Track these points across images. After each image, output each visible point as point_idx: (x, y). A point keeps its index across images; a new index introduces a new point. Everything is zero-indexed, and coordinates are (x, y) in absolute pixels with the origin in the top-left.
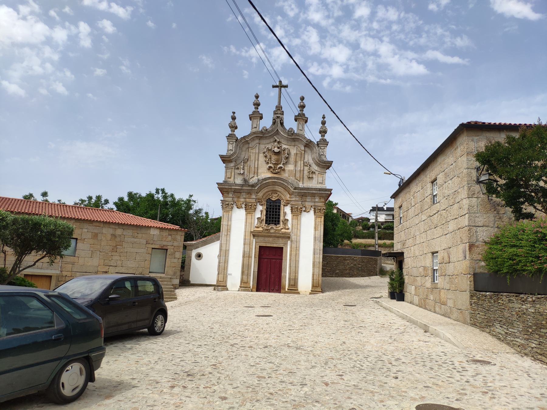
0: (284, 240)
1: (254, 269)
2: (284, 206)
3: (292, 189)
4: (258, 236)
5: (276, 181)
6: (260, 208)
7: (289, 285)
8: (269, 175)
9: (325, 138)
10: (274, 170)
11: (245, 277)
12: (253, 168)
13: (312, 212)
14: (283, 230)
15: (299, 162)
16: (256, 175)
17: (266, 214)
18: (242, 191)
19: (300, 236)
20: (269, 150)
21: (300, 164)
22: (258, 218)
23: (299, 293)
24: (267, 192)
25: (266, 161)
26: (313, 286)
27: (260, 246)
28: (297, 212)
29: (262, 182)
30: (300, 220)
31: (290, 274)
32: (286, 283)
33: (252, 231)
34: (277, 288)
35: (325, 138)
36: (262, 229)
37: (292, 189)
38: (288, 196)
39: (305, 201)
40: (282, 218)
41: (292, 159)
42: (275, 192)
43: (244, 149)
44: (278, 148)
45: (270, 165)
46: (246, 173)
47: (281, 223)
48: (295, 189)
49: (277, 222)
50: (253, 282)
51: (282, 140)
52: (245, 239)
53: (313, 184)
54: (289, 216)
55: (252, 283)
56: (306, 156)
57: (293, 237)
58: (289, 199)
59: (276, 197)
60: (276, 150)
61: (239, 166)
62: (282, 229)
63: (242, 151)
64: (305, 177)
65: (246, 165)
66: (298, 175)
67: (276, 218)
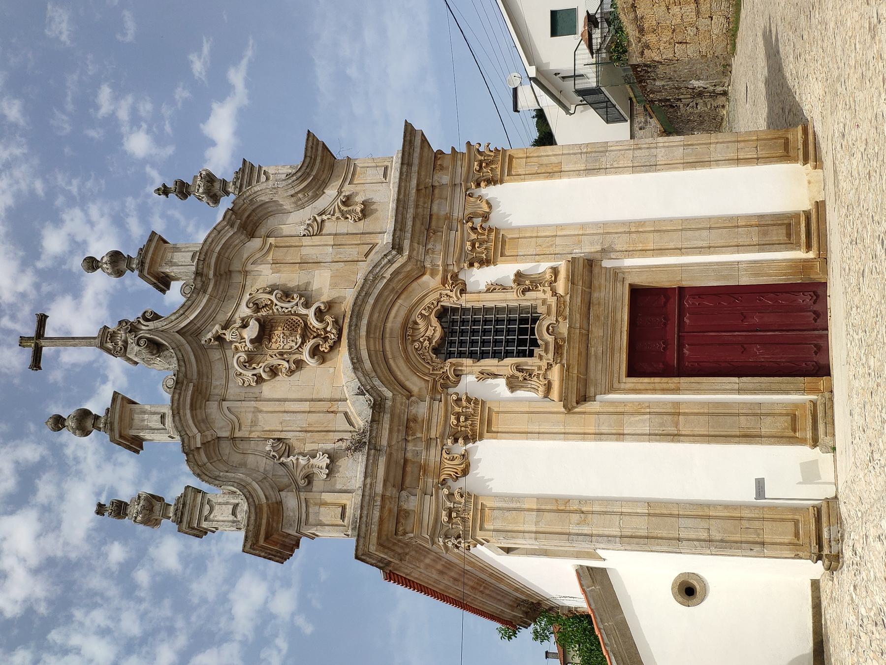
0: (601, 281)
2: (463, 291)
3: (401, 260)
5: (365, 322)
6: (469, 384)
7: (790, 243)
8: (343, 356)
9: (230, 178)
10: (326, 339)
11: (767, 426)
12: (313, 418)
13: (489, 192)
14: (561, 286)
15: (304, 251)
16: (341, 407)
17: (496, 355)
18: (398, 456)
19: (583, 226)
20: (250, 360)
21: (312, 248)
22: (512, 385)
23: (820, 206)
24: (407, 359)
25: (291, 372)
26: (786, 154)
27: (631, 373)
28: (488, 245)
29: (365, 374)
30: (519, 229)
31: (739, 247)
32: (775, 261)
34: (804, 300)
35: (230, 178)
36: (556, 369)
37: (401, 260)
38: (430, 282)
39: (448, 218)
41: (291, 278)
42: (408, 329)
43: (236, 458)
44: (245, 326)
45: (305, 356)
46: (329, 446)
48: (397, 246)
50: (787, 392)
51: (222, 318)
53: (385, 197)
54: (503, 271)
55: (789, 396)
56: (286, 229)
57: (587, 248)
58: (439, 277)
59: (429, 324)
60: (252, 331)
61: (299, 475)
62: (554, 293)
63: (243, 465)
65: (297, 446)
66: (353, 252)
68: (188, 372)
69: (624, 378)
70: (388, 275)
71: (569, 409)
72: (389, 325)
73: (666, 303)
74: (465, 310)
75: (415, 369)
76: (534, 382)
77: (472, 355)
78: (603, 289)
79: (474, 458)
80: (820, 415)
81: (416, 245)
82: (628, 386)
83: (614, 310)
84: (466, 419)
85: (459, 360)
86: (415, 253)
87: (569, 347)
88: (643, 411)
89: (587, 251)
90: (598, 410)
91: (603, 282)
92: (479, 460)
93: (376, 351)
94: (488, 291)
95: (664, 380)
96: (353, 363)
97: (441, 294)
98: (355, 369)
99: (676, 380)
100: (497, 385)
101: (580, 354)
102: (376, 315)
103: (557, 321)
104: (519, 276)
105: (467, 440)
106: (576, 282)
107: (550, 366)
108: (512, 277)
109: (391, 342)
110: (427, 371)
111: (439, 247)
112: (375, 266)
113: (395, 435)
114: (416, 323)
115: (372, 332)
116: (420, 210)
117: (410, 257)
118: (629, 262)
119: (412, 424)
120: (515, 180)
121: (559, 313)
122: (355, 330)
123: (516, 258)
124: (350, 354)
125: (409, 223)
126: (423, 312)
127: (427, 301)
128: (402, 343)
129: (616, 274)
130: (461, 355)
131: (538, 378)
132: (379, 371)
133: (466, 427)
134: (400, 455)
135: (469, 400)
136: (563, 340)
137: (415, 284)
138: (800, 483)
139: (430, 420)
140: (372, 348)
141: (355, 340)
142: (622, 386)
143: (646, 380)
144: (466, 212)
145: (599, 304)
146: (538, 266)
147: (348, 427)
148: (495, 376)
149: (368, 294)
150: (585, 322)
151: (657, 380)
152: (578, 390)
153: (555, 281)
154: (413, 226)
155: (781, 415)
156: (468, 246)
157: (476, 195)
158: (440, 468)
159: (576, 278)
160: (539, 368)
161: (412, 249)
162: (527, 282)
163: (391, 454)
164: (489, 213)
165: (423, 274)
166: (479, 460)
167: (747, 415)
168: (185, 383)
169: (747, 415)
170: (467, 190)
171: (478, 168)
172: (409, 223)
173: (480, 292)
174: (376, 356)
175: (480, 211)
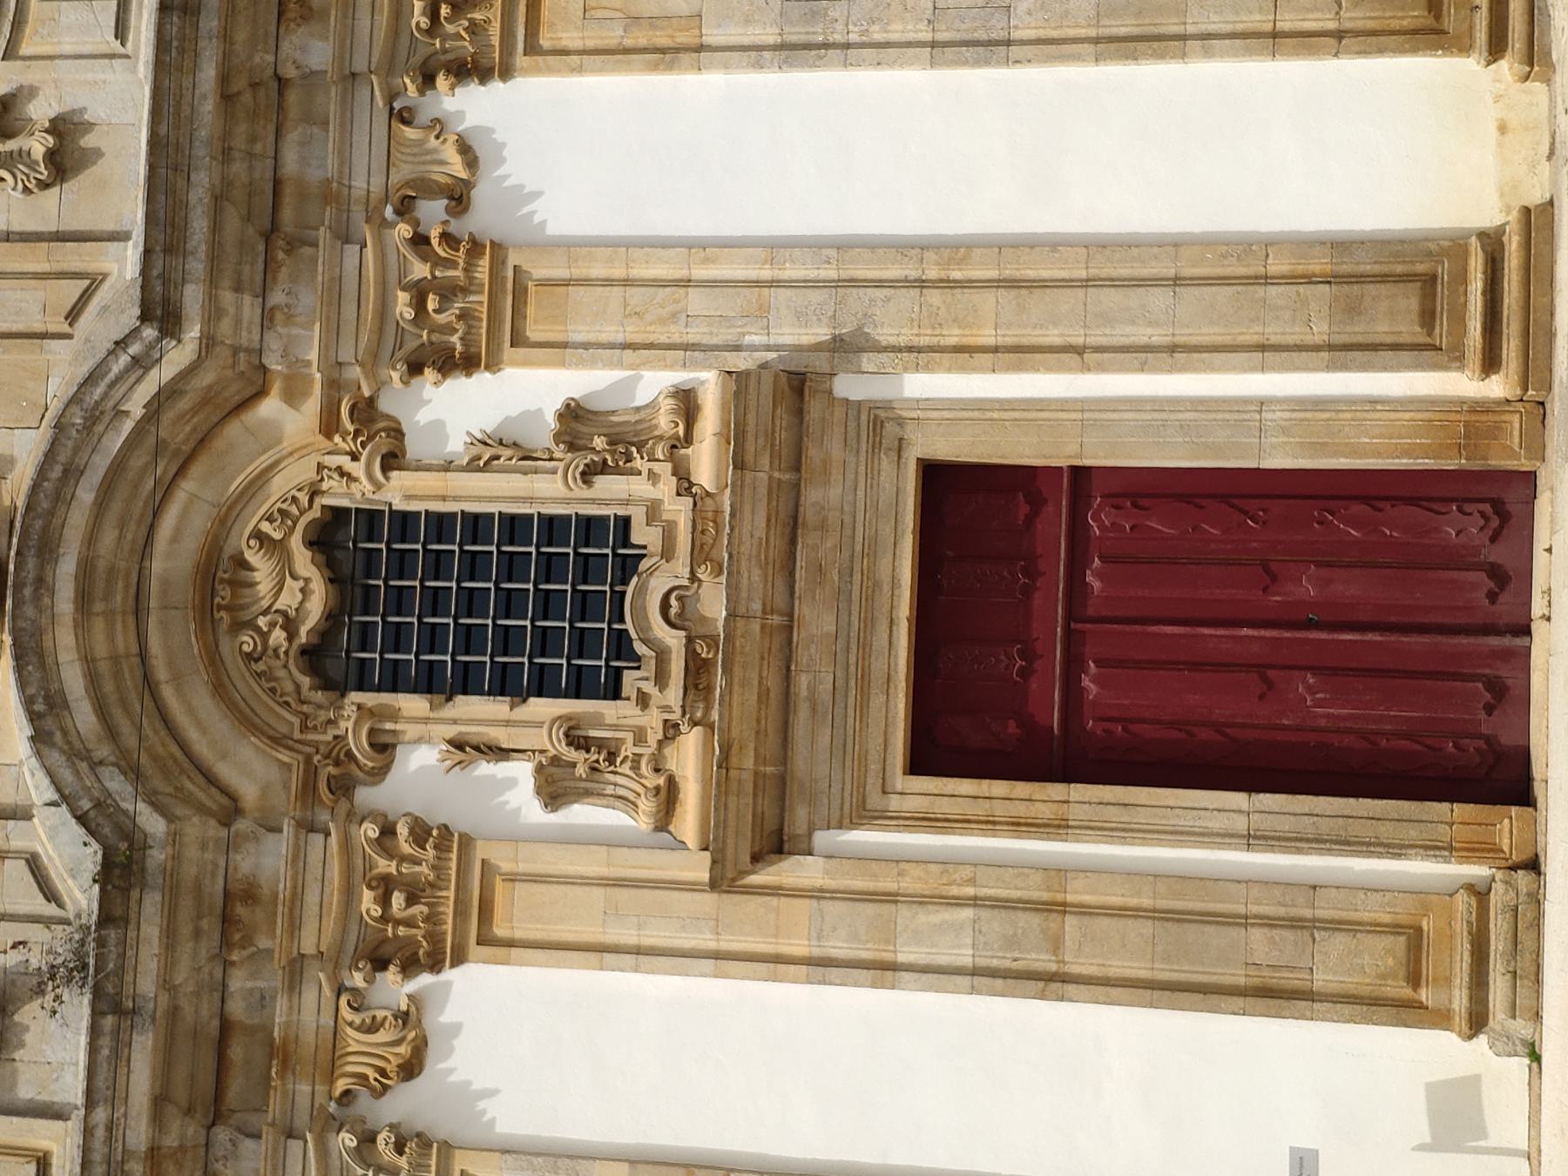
0: (827, 448)
1: (1226, 838)
3: (177, 357)
4: (779, 786)
5: (66, 568)
11: (1332, 964)
13: (469, 105)
14: (705, 461)
19: (775, 247)
24: (220, 689)
27: (918, 764)
28: (471, 301)
29: (77, 753)
30: (571, 246)
33: (698, 867)
36: (691, 742)
37: (177, 357)
38: (288, 420)
39: (332, 195)
40: (548, 492)
42: (218, 581)
47: (610, 494)
48: (160, 311)
49: (593, 556)
52: (821, 966)
57: (793, 330)
58: (313, 405)
59: (286, 568)
62: (685, 483)
64: (48, 210)
67: (550, 567)
69: (901, 781)
70: (136, 407)
71: (721, 881)
72: (157, 566)
73: (1030, 521)
74: (404, 522)
75: (248, 722)
76: (621, 780)
77: (430, 683)
78: (836, 475)
79: (442, 1017)
80: (1498, 944)
81: (227, 297)
82: (912, 804)
83: (871, 550)
84: (411, 900)
85: (386, 698)
86: (225, 326)
87: (730, 684)
88: (955, 891)
89: (788, 340)
90: (819, 883)
91: (836, 451)
92: (456, 1029)
93: (115, 659)
94: (473, 466)
95: (1022, 788)
96: (33, 717)
97: (320, 467)
98: (39, 739)
99: (1056, 790)
100: (511, 783)
101: (763, 697)
102: (108, 537)
103: (693, 577)
104: (574, 416)
105: (410, 967)
106: (749, 458)
107: (671, 730)
108: (551, 422)
109: (164, 625)
110: (284, 729)
111: (308, 300)
112: (91, 380)
113: (185, 949)
114: (243, 564)
115: (99, 589)
116: (238, 168)
117: (208, 343)
118: (921, 385)
119: (240, 910)
120: (551, 71)
121: (699, 554)
123: (559, 349)
124: (22, 683)
125: (199, 225)
126: (266, 527)
127: (280, 485)
128: (201, 632)
129: (877, 425)
130: (395, 681)
131: (636, 767)
133: (409, 923)
134: (207, 1008)
135: (420, 832)
136: (712, 641)
137: (233, 429)
138: (1422, 1147)
139: (297, 898)
140: (101, 650)
141: (38, 633)
142: (894, 803)
143: (966, 786)
144: (395, 178)
145: (823, 526)
146: (629, 385)
147: (38, 904)
148: (500, 753)
149: (73, 473)
150: (780, 585)
151: (999, 787)
152: (758, 819)
153: (688, 439)
154: (216, 227)
155: (1376, 928)
156: (402, 305)
157: (424, 117)
158: (331, 1059)
159: (750, 446)
160: (640, 737)
161: (213, 313)
162: (599, 442)
163: (174, 1012)
164: (468, 185)
165: (261, 393)
166: (456, 1029)
167: (1270, 922)
169: (1270, 922)
170: (391, 98)
171: (425, 22)
172: (199, 225)
173: (448, 467)
174: (117, 675)
175: (438, 175)
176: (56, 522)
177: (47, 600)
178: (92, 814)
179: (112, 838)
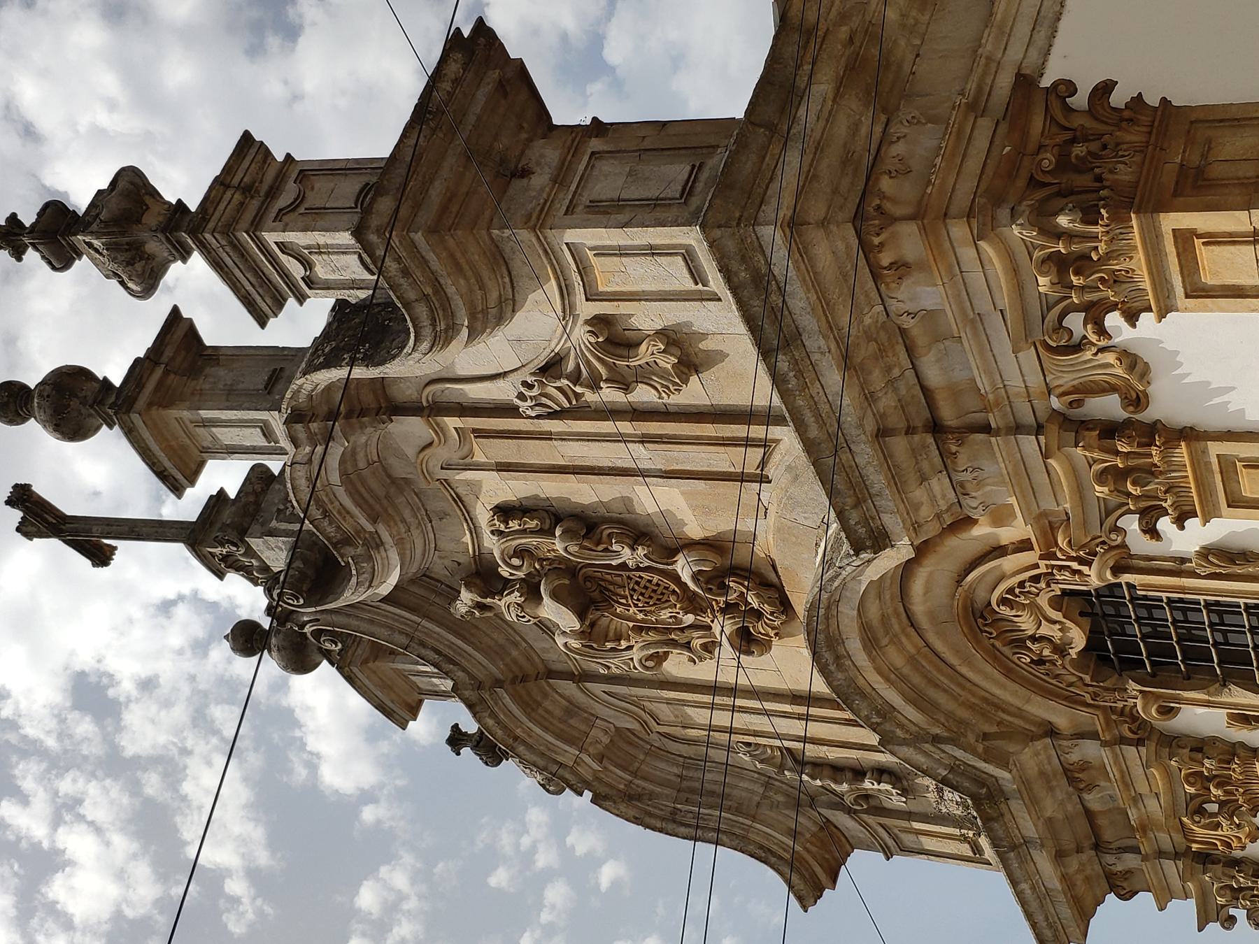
68: (475, 671)
122: (840, 667)
132: (941, 699)
140: (898, 660)
168: (486, 696)
176: (833, 626)
177: (848, 663)
178: (950, 776)
179: (974, 789)
